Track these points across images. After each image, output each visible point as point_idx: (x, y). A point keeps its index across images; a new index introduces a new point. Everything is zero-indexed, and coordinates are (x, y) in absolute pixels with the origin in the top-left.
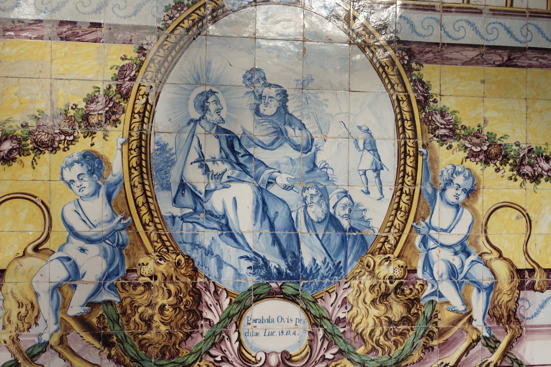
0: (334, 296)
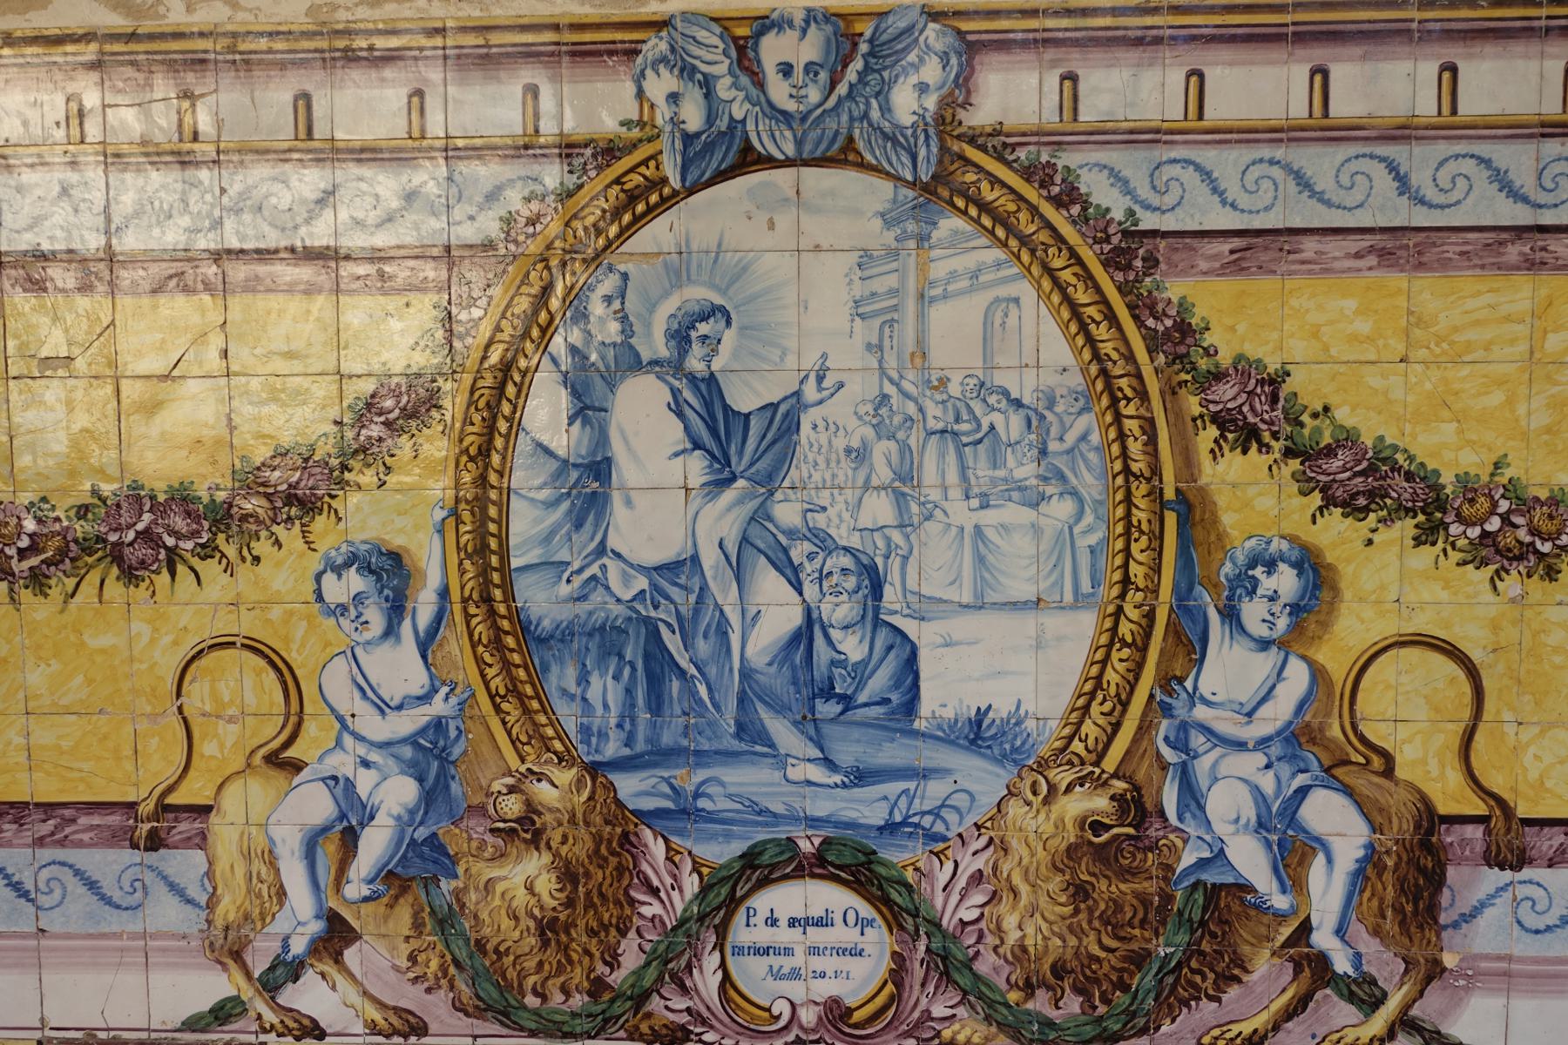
0: (949, 866)
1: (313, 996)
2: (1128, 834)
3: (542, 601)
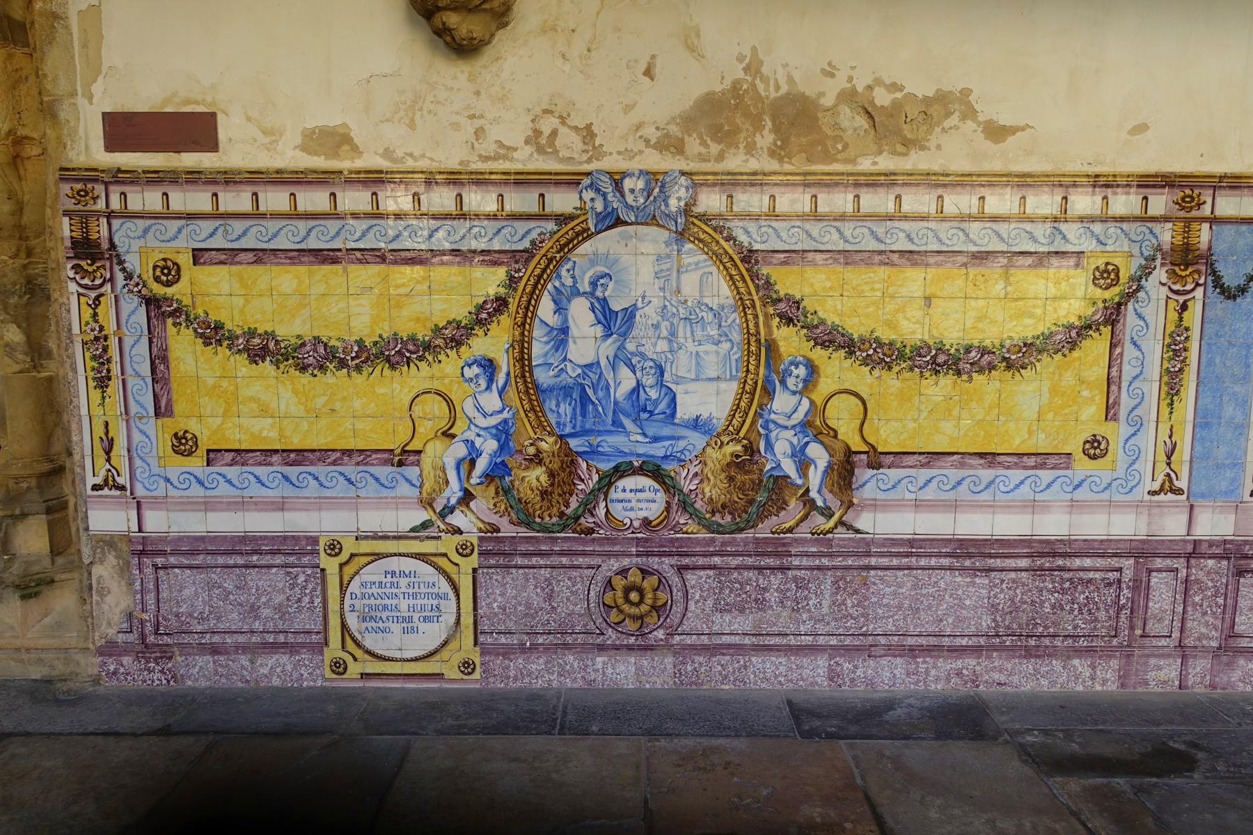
1: (458, 519)
2: (747, 459)
3: (544, 377)
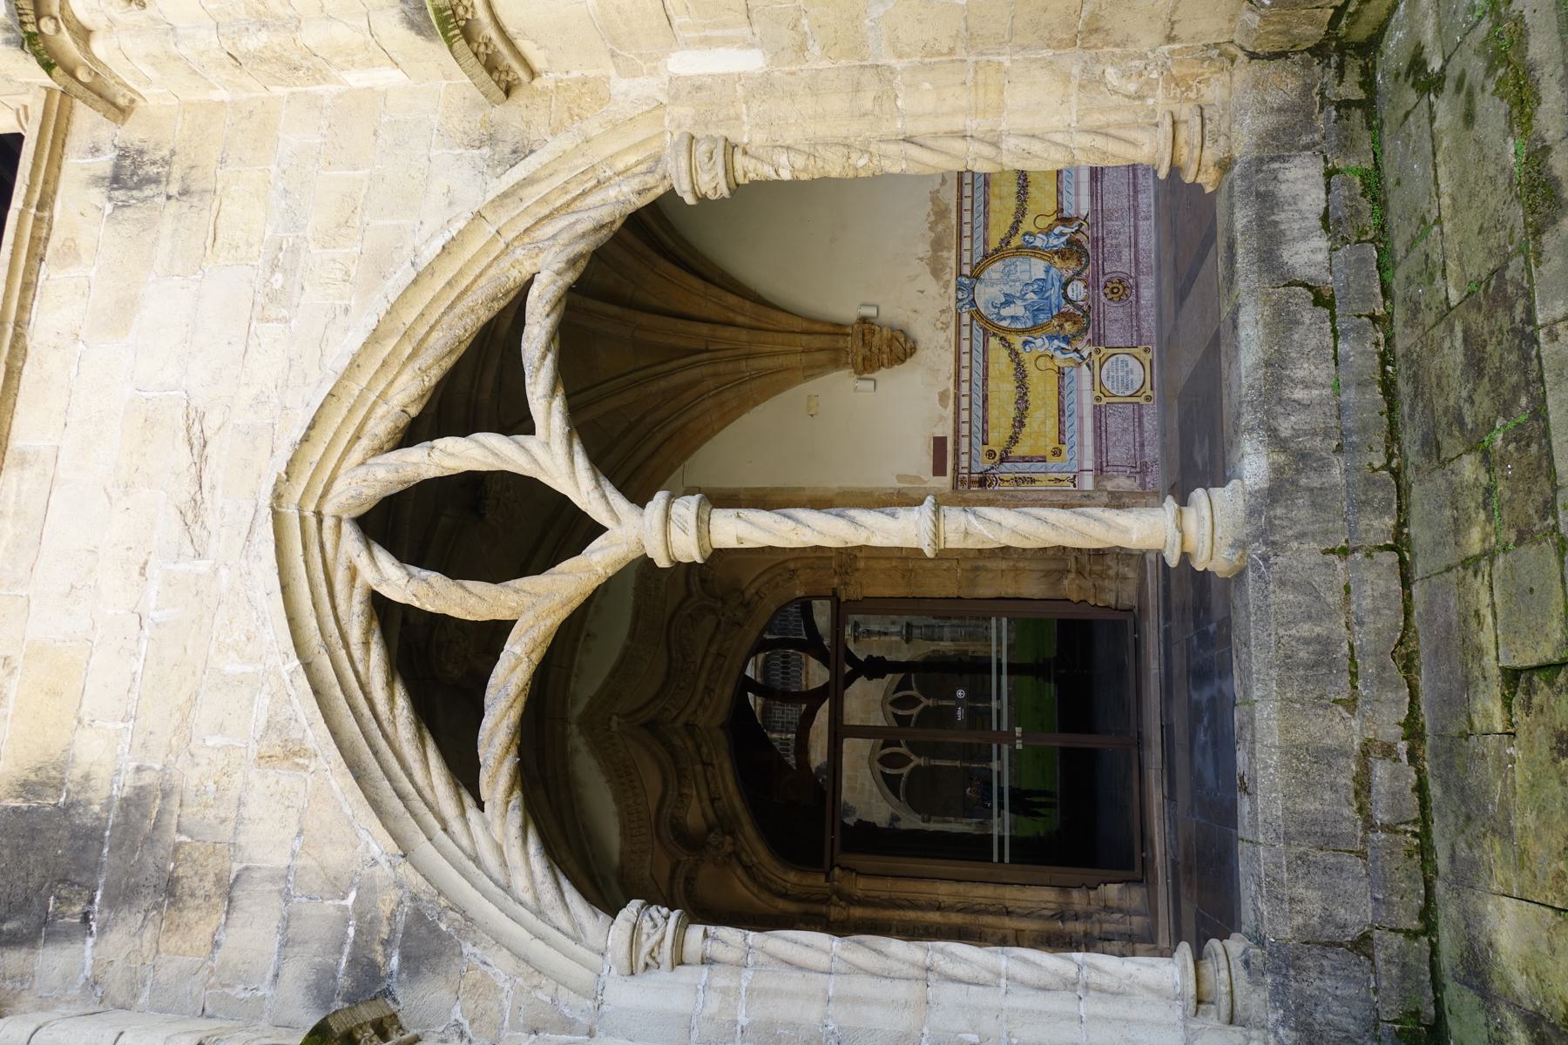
1: (1085, 354)
3: (1030, 324)
